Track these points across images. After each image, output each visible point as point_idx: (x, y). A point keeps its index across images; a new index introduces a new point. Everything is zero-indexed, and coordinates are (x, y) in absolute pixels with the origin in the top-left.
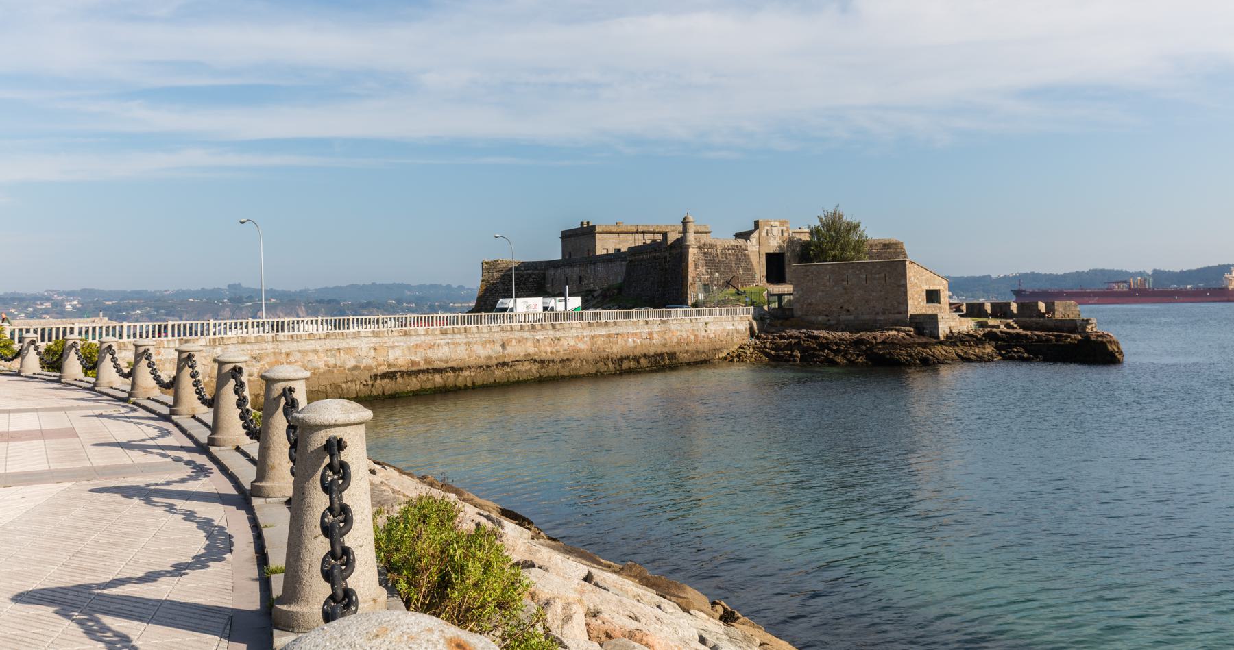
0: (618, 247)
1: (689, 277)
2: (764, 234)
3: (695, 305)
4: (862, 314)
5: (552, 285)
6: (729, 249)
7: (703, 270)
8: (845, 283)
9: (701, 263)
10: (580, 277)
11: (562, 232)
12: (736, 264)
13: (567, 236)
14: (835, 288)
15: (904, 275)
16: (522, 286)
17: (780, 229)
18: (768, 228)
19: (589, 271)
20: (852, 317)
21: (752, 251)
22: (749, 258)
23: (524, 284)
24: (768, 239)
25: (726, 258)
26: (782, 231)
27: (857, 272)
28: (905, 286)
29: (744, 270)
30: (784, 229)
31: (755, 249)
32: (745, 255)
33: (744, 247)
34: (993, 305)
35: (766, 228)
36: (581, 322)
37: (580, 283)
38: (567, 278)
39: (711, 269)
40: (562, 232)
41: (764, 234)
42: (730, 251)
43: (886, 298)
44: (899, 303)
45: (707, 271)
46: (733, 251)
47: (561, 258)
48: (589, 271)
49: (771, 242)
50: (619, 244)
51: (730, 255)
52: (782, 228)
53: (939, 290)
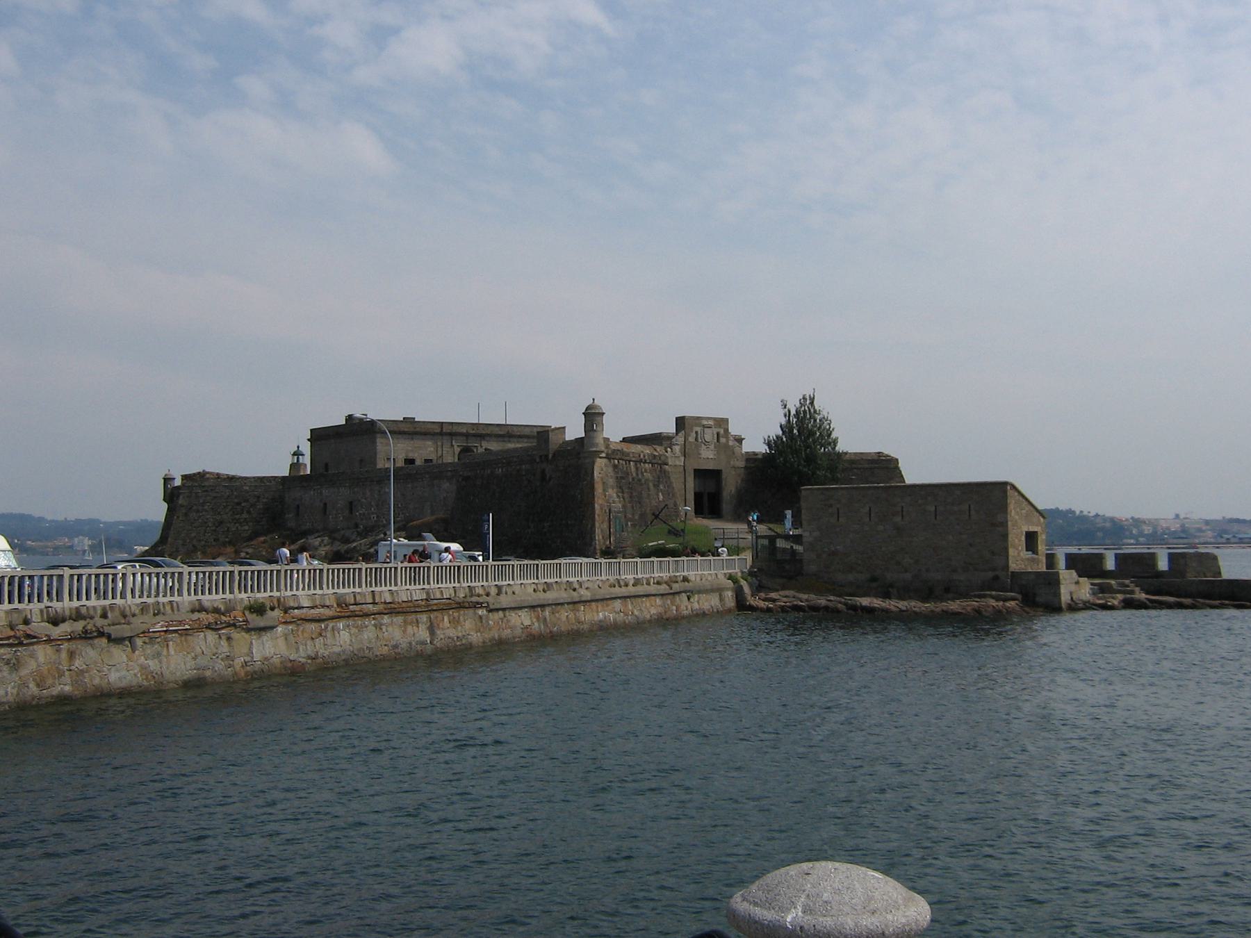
0: (411, 456)
1: (596, 505)
2: (691, 439)
3: (607, 553)
4: (928, 570)
5: (298, 514)
7: (612, 493)
8: (898, 519)
9: (611, 481)
10: (351, 503)
11: (311, 430)
13: (319, 437)
14: (881, 528)
15: (1004, 508)
16: (245, 516)
17: (715, 430)
19: (368, 493)
20: (908, 576)
23: (249, 512)
24: (698, 447)
25: (642, 473)
26: (718, 434)
27: (920, 502)
28: (1004, 524)
30: (722, 431)
31: (678, 463)
32: (665, 471)
34: (1172, 558)
35: (698, 429)
36: (536, 581)
37: (351, 511)
38: (325, 504)
39: (623, 493)
40: (311, 430)
41: (691, 439)
43: (971, 545)
44: (993, 553)
45: (618, 496)
47: (288, 475)
48: (368, 493)
49: (702, 452)
50: (412, 451)
51: (646, 471)
53: (1037, 532)
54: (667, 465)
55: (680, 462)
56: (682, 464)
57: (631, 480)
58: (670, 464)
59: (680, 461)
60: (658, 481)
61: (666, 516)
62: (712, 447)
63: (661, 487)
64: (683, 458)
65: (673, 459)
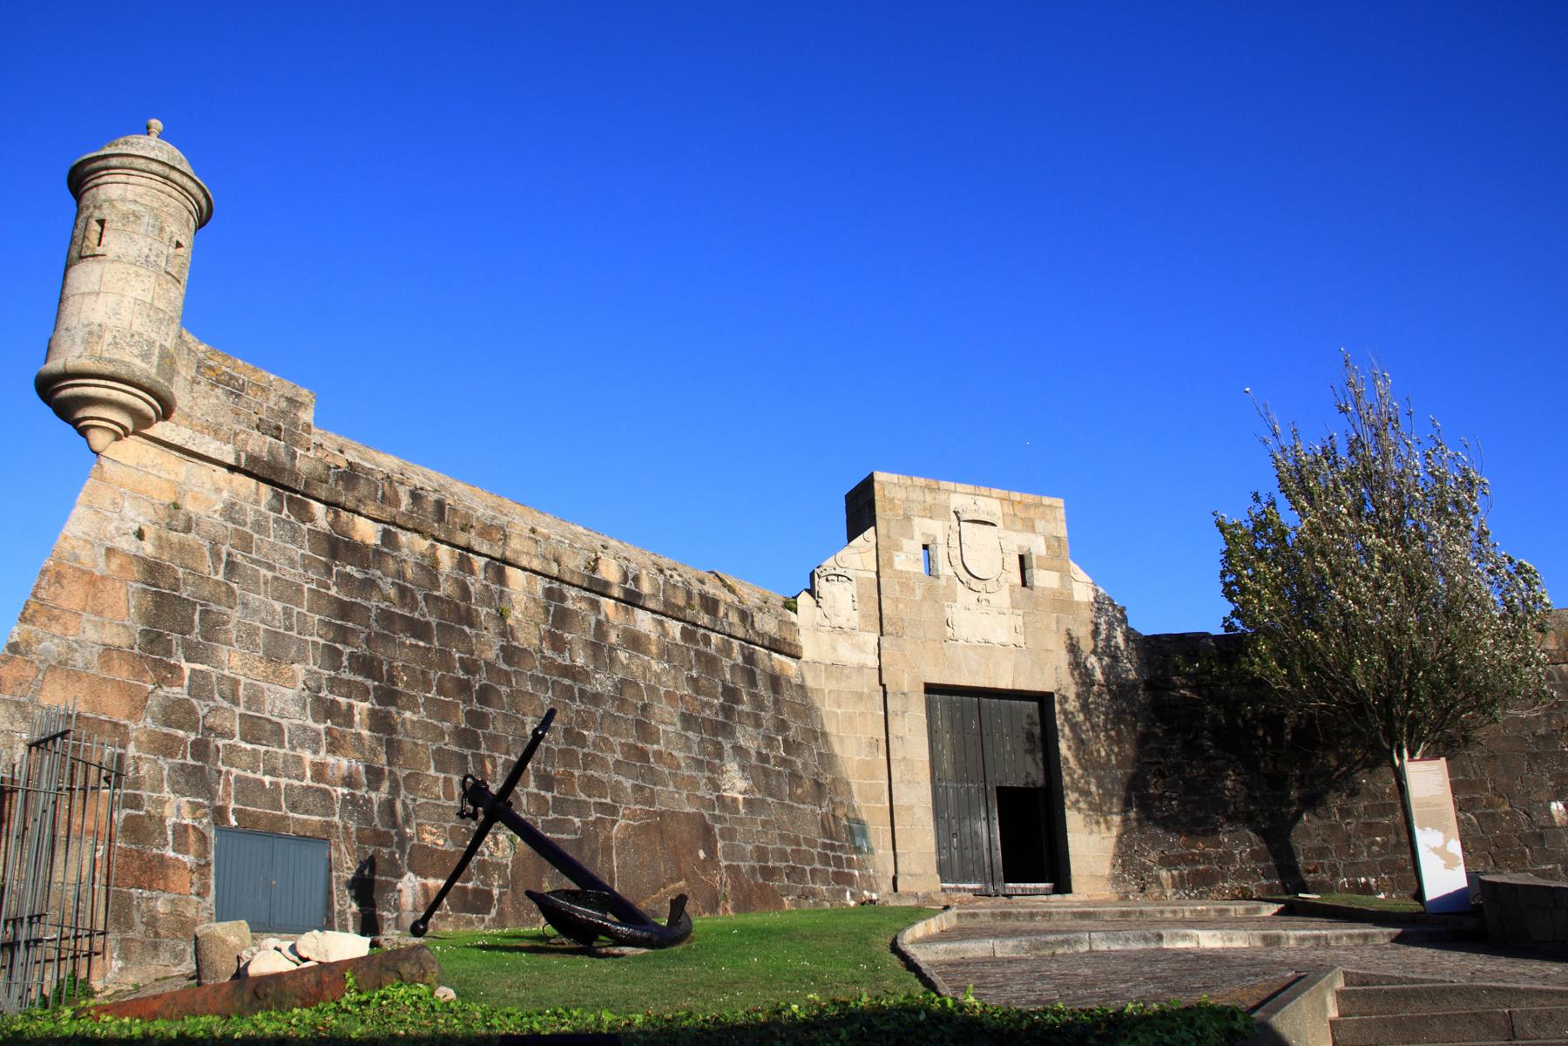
2: (907, 560)
6: (632, 600)
12: (688, 720)
18: (936, 528)
21: (835, 668)
22: (807, 710)
29: (759, 771)
31: (846, 653)
32: (775, 681)
33: (767, 624)
35: (925, 527)
41: (907, 560)
42: (644, 622)
46: (675, 628)
49: (955, 613)
51: (635, 641)
52: (1018, 541)
54: (797, 657)
55: (860, 651)
56: (872, 661)
57: (491, 654)
58: (807, 654)
59: (859, 648)
60: (727, 711)
61: (768, 873)
62: (1002, 598)
63: (747, 738)
64: (873, 638)
65: (824, 637)
